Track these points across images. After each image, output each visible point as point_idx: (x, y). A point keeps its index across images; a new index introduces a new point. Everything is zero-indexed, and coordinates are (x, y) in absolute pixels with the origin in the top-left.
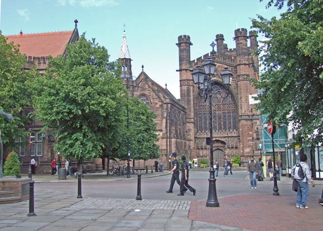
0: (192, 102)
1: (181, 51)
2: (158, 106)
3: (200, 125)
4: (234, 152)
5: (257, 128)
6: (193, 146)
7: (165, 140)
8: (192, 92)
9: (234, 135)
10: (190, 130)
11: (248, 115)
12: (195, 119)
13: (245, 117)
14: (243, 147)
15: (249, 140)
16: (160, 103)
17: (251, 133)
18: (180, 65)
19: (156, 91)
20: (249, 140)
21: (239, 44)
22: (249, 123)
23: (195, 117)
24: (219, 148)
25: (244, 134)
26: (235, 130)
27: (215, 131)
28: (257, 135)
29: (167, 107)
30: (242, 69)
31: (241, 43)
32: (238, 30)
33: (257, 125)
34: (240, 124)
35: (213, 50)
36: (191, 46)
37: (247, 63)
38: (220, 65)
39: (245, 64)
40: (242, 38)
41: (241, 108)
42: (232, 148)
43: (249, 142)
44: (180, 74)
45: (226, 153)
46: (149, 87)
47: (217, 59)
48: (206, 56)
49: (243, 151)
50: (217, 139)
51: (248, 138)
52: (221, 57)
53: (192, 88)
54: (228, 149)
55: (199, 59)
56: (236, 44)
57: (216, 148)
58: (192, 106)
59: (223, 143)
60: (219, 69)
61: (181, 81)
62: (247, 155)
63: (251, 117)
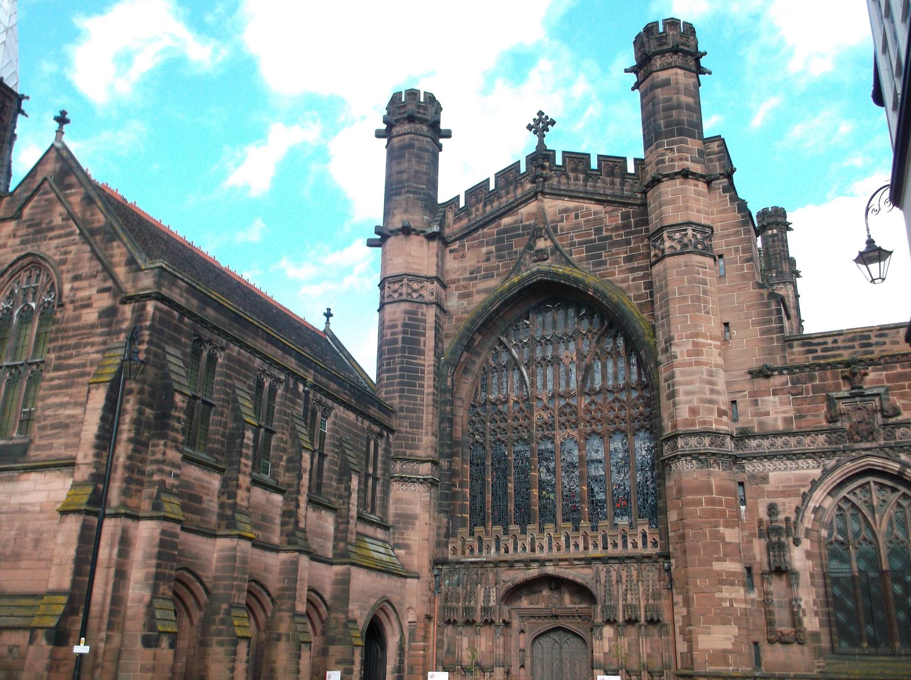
0: (428, 383)
1: (393, 155)
2: (90, 316)
3: (473, 498)
4: (645, 648)
5: (772, 509)
6: (423, 610)
7: (73, 525)
8: (430, 334)
9: (640, 550)
10: (407, 519)
11: (716, 434)
12: (444, 463)
13: (693, 441)
14: (688, 620)
15: (725, 580)
16: (104, 301)
17: (731, 535)
18: (387, 213)
19: (93, 232)
20: (725, 580)
21: (653, 87)
22: (718, 476)
23: (441, 455)
24: (561, 622)
25: (688, 544)
26: (644, 526)
27: (542, 530)
28: (770, 547)
29: (139, 314)
30: (674, 201)
31: (666, 83)
32: (650, 29)
33: (768, 487)
34: (670, 483)
35: (541, 143)
36: (441, 141)
37: (697, 168)
38: (571, 204)
39: (685, 174)
40: (669, 59)
41: (672, 395)
42: (631, 622)
43: (726, 592)
44: (384, 254)
45: (598, 655)
46: (70, 216)
47: (555, 181)
48: (508, 176)
49: (690, 641)
50: (550, 569)
51: (717, 566)
52: (575, 170)
53: (431, 314)
54: (608, 631)
55: (477, 193)
56: (643, 96)
57: (553, 623)
58: (428, 400)
59: (582, 591)
60: (564, 224)
61: (382, 286)
62: (710, 669)
63: (730, 446)
